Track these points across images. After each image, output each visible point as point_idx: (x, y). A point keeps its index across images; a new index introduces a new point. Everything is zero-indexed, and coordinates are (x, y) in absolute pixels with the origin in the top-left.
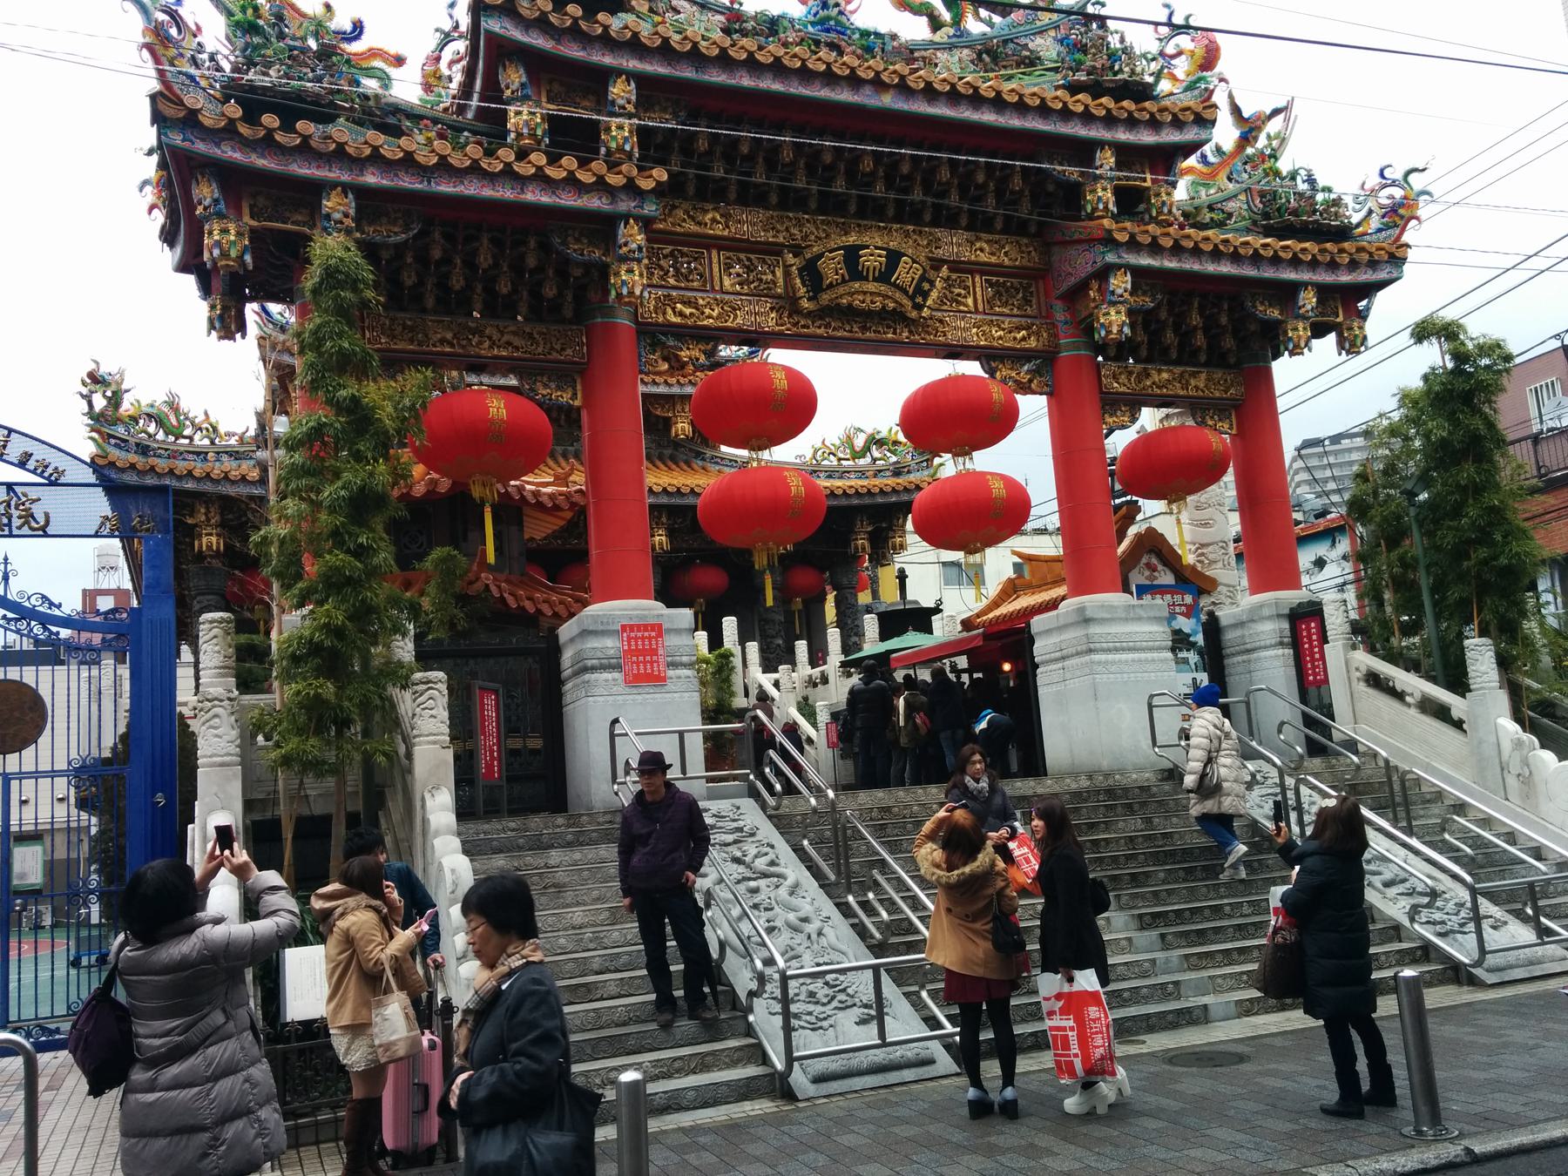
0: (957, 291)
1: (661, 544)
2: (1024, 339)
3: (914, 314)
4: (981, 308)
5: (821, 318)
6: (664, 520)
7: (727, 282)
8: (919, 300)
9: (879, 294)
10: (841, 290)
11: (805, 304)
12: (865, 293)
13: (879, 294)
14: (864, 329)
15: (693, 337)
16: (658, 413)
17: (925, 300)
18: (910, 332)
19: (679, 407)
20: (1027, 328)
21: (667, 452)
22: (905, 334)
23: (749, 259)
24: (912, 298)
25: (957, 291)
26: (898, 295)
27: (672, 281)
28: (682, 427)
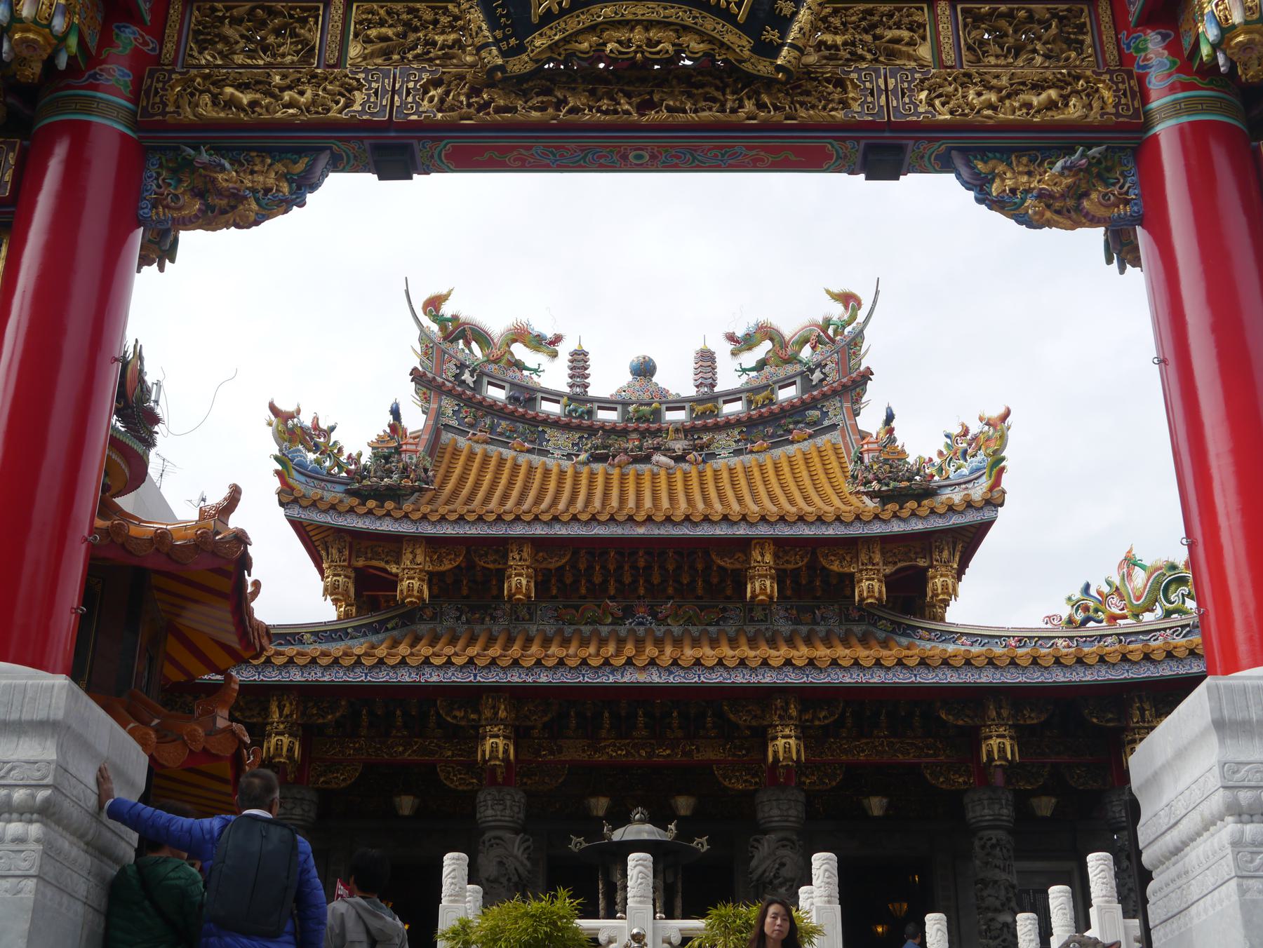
0: (889, 34)
1: (787, 750)
2: (1051, 105)
3: (763, 67)
4: (949, 57)
5: (548, 92)
6: (793, 712)
7: (354, 50)
8: (771, 35)
9: (664, 25)
10: (572, 24)
11: (493, 57)
12: (630, 25)
13: (664, 25)
14: (643, 108)
15: (264, 151)
16: (835, 567)
17: (783, 35)
18: (761, 106)
19: (863, 557)
20: (1059, 84)
21: (858, 629)
22: (749, 106)
23: (411, 11)
24: (751, 27)
25: (889, 34)
26: (710, 24)
27: (239, 59)
28: (870, 587)
